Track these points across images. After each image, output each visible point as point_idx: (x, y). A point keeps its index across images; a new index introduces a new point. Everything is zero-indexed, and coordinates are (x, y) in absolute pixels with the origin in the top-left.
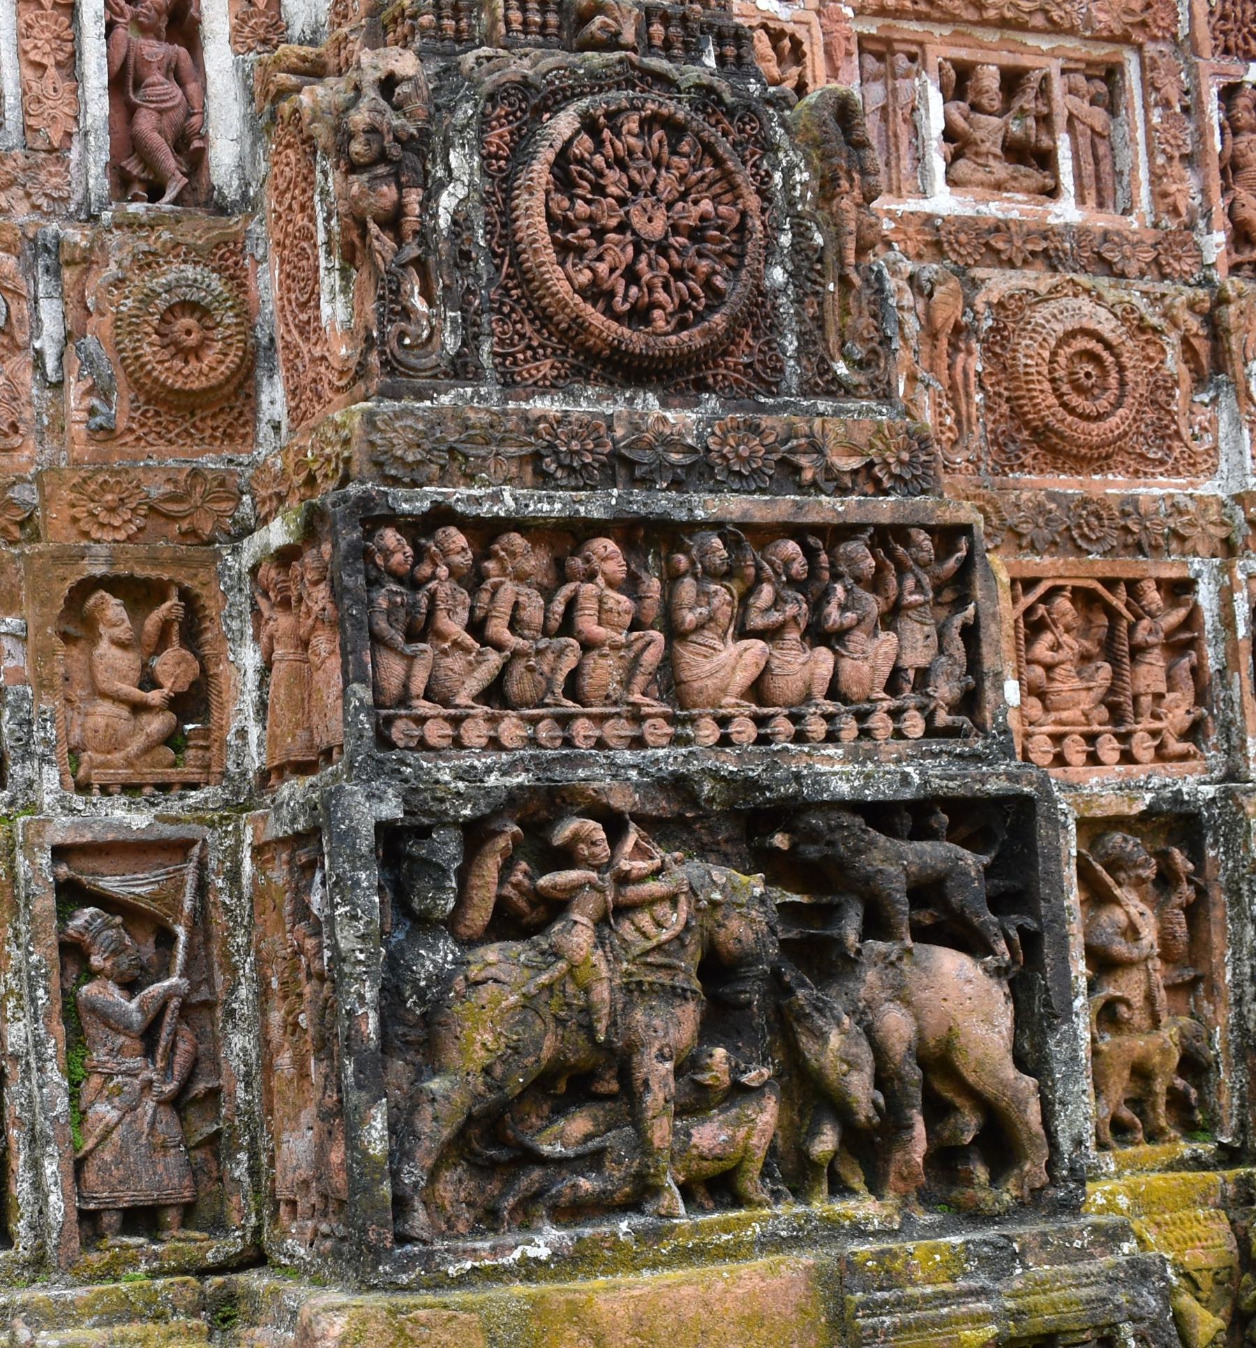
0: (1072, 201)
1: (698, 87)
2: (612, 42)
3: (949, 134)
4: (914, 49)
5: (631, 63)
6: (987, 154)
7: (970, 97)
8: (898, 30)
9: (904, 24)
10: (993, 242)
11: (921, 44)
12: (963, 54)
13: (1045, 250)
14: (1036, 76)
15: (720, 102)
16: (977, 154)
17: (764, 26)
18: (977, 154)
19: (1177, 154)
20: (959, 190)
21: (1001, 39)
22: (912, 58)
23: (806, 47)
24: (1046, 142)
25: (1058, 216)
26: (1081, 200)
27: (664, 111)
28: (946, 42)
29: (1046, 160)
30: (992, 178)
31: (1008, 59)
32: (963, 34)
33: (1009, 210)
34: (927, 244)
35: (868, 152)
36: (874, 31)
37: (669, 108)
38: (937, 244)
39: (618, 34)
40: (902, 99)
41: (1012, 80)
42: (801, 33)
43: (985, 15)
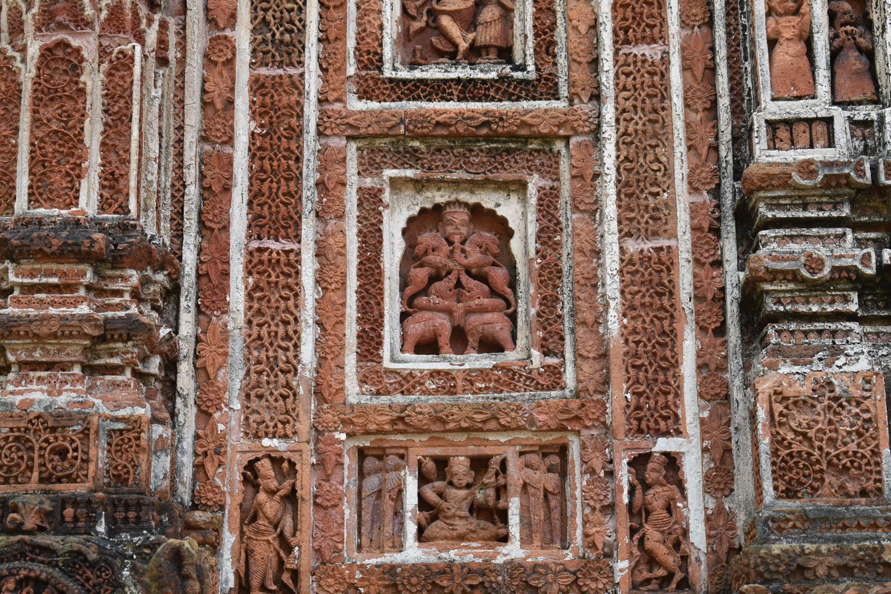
0: (518, 544)
1: (71, 552)
2: (18, 529)
3: (423, 503)
4: (402, 451)
5: (25, 542)
6: (454, 516)
7: (448, 477)
8: (388, 441)
9: (393, 437)
10: (438, 582)
11: (406, 448)
12: (438, 451)
13: (482, 583)
14: (498, 459)
15: (86, 560)
16: (447, 518)
17: (269, 456)
18: (447, 518)
19: (598, 506)
20: (426, 544)
21: (468, 438)
22: (402, 457)
23: (298, 467)
24: (501, 504)
25: (505, 555)
26: (526, 541)
27: (32, 574)
28: (423, 445)
29: (503, 515)
30: (455, 534)
31: (473, 450)
32: (438, 438)
33: (465, 554)
34: (386, 587)
35: (191, 582)
36: (368, 444)
37: (39, 570)
38: (395, 585)
39: (22, 524)
40: (389, 486)
41: (479, 464)
42: (295, 458)
43: (447, 427)
